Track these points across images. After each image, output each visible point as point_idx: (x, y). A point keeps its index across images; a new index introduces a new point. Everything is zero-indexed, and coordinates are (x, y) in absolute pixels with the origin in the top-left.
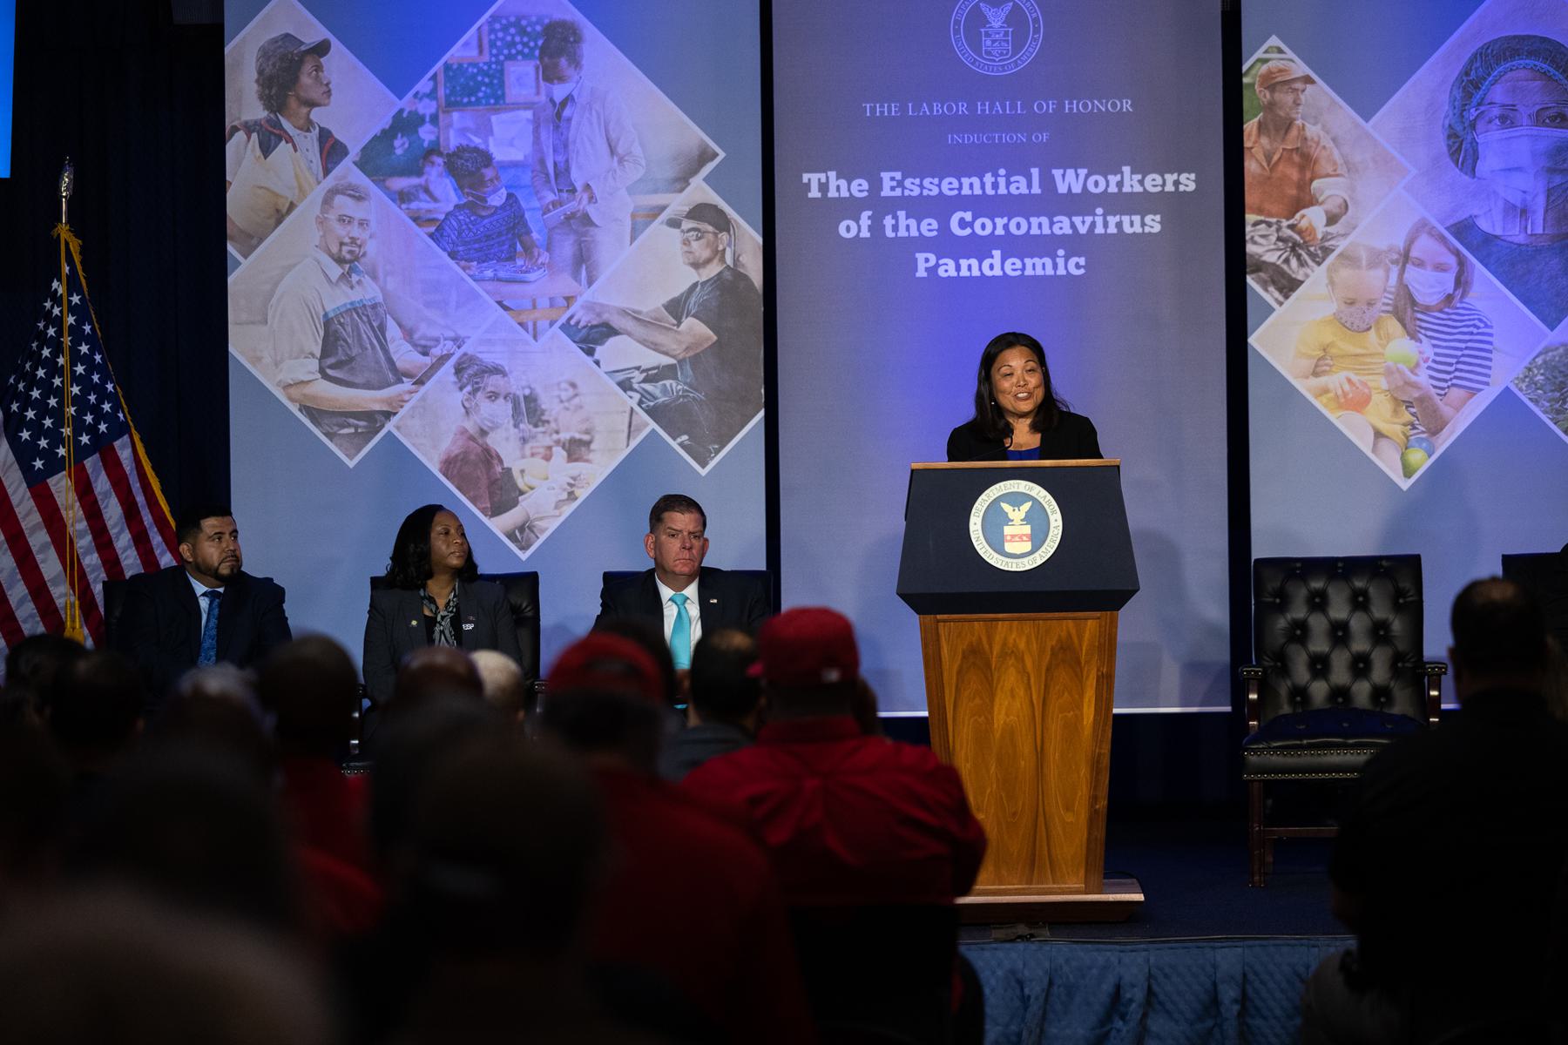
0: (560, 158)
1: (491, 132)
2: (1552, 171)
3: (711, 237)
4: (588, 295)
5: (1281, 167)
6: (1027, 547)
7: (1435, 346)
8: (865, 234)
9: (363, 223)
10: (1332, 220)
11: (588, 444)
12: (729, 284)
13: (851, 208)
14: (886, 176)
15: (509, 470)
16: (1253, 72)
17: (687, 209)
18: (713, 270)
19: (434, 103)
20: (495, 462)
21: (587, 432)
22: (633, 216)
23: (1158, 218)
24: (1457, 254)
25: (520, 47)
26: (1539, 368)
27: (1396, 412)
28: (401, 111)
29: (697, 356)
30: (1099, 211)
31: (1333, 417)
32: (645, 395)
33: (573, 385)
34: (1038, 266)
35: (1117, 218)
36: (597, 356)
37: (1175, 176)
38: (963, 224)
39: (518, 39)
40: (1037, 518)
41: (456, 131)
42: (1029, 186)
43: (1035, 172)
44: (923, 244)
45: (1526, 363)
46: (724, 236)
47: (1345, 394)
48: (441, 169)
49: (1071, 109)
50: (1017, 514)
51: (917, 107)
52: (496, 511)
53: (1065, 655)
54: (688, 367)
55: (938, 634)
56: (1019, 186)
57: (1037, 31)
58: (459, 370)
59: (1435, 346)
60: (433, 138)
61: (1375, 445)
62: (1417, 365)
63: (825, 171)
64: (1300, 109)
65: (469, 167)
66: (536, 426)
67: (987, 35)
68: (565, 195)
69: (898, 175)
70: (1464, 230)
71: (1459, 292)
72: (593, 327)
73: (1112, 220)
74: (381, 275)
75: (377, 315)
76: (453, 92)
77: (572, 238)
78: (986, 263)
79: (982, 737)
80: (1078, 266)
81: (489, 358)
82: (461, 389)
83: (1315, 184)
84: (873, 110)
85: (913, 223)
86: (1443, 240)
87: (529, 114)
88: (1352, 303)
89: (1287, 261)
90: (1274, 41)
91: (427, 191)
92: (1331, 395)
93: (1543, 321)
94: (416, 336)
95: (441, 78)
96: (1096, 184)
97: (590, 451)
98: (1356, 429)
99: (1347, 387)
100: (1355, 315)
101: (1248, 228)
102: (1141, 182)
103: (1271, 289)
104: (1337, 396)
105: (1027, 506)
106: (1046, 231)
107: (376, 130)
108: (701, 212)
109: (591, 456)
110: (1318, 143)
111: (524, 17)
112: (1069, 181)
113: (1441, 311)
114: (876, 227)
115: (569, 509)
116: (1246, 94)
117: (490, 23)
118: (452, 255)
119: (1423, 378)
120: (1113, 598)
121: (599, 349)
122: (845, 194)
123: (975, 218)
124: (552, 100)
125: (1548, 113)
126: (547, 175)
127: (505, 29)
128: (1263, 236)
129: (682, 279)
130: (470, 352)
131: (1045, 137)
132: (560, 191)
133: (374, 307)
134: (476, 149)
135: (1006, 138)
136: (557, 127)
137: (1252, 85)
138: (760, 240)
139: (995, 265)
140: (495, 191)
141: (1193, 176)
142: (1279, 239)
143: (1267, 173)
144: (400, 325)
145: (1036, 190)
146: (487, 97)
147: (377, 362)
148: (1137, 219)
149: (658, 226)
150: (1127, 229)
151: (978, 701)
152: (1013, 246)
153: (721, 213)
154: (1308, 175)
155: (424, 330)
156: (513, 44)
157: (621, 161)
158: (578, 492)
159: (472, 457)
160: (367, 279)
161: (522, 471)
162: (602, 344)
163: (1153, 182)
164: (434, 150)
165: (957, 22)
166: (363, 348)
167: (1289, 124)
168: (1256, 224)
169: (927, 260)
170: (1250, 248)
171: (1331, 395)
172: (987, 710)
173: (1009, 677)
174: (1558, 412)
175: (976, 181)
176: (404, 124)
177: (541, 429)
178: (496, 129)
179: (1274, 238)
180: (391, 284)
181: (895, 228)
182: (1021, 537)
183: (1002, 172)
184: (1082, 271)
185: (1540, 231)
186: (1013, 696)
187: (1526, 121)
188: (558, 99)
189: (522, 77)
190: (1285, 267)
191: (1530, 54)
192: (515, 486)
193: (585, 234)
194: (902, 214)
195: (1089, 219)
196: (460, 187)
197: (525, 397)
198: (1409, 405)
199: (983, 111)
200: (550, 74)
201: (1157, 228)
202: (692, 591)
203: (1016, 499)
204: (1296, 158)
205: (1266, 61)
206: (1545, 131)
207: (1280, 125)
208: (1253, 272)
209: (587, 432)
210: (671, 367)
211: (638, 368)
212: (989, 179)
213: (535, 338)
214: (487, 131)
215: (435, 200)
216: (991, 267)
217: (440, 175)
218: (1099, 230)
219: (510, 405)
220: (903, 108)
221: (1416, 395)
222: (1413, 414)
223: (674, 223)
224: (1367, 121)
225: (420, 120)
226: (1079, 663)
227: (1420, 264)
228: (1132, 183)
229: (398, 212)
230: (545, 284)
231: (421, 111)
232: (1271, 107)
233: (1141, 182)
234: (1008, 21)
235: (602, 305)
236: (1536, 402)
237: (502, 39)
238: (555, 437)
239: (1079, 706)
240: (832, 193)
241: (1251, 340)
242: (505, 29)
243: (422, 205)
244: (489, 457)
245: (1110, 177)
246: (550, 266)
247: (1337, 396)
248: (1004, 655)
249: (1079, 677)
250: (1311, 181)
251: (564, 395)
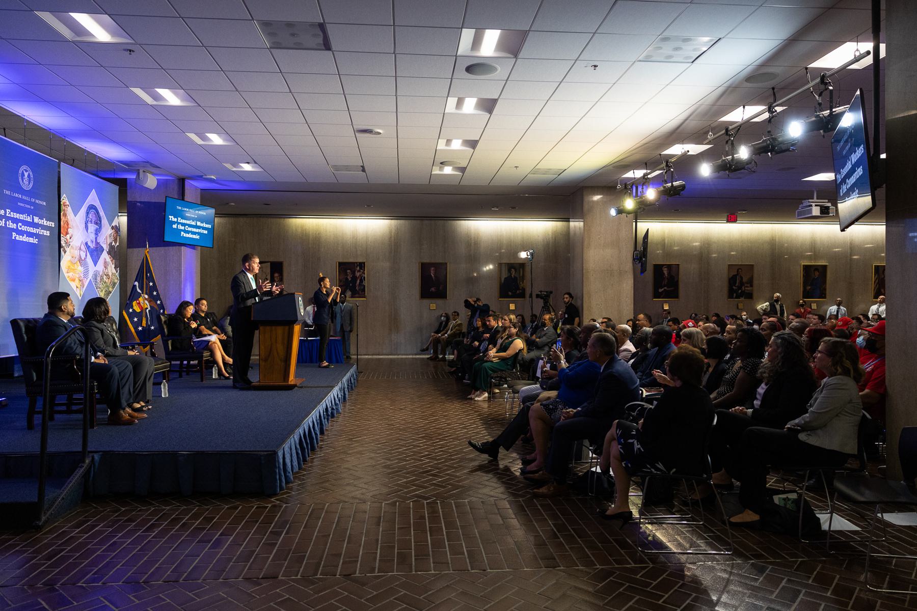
34: (31, 240)
56: (29, 219)
70: (86, 244)
112: (36, 220)
114: (5, 224)
139: (24, 239)
207: (65, 215)
228: (45, 222)
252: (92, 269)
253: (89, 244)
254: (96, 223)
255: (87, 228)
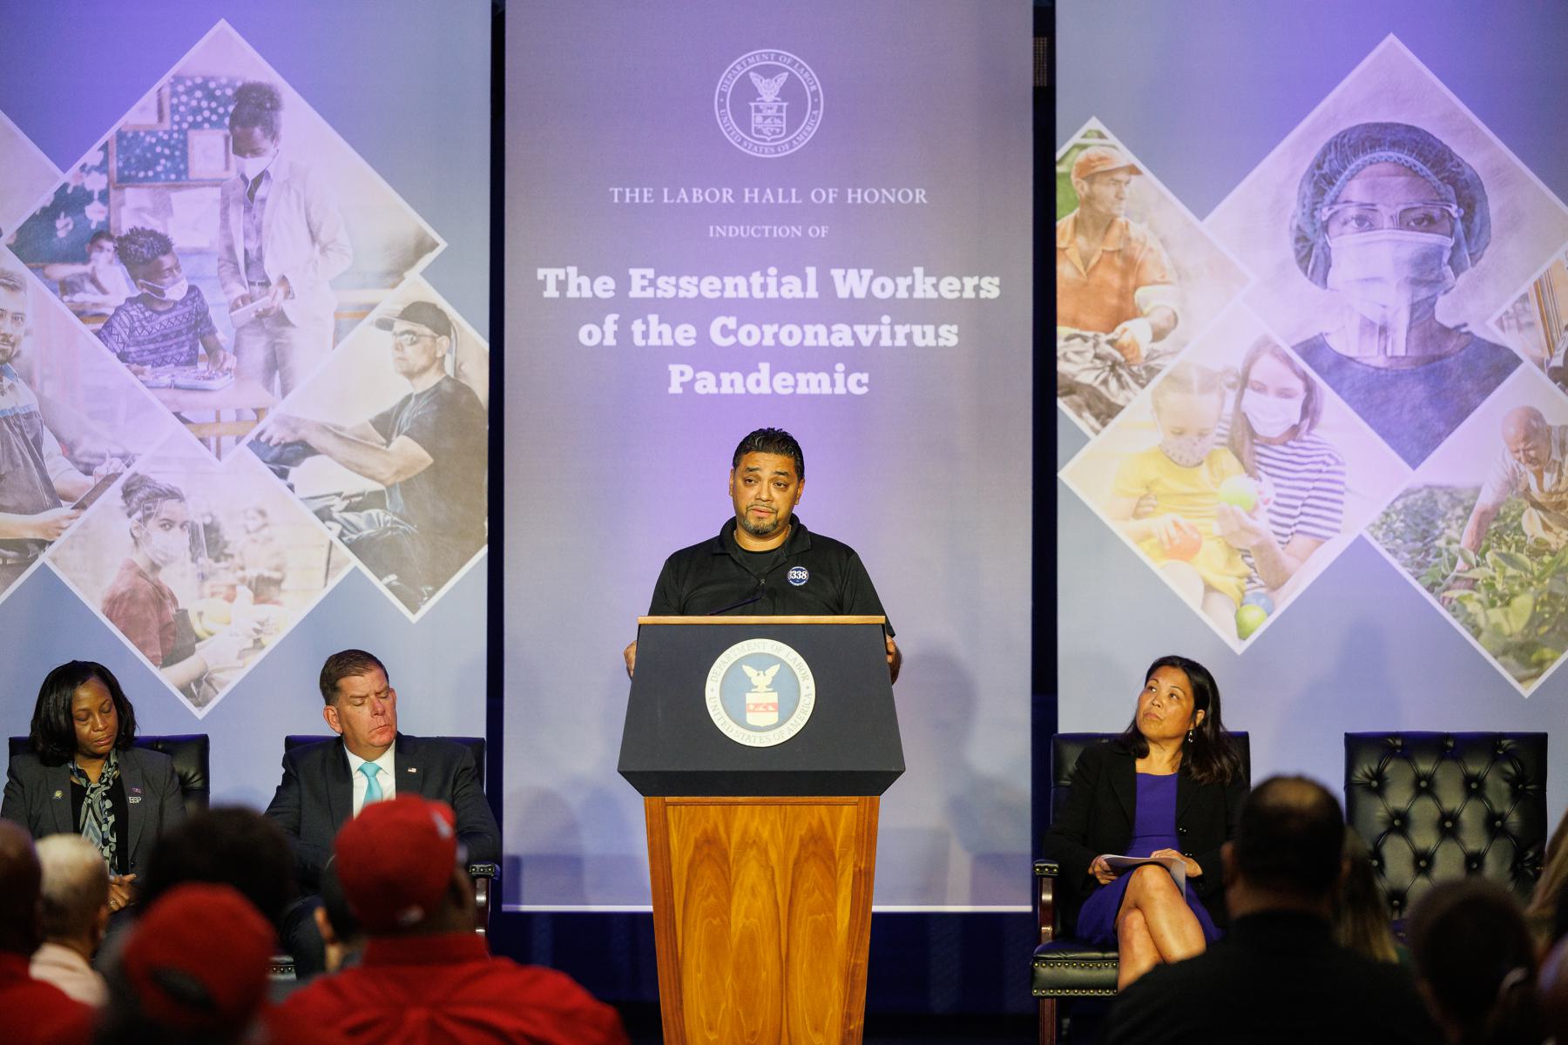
0: (252, 246)
1: (171, 211)
2: (1416, 282)
3: (428, 341)
4: (280, 408)
5: (1099, 272)
6: (773, 718)
7: (1277, 485)
8: (610, 341)
9: (17, 317)
10: (1158, 335)
11: (278, 582)
12: (448, 398)
13: (594, 310)
14: (635, 273)
15: (183, 614)
16: (1069, 159)
17: (400, 308)
18: (430, 380)
19: (104, 178)
20: (168, 602)
21: (278, 569)
22: (337, 315)
23: (955, 329)
24: (1304, 377)
25: (206, 114)
26: (1398, 513)
27: (1229, 562)
28: (65, 186)
29: (408, 482)
30: (886, 319)
31: (1159, 566)
32: (347, 527)
33: (262, 513)
35: (907, 328)
36: (291, 479)
37: (976, 280)
38: (725, 331)
39: (204, 104)
40: (785, 685)
41: (133, 210)
42: (804, 288)
43: (811, 272)
44: (677, 354)
45: (1383, 508)
46: (444, 340)
47: (1171, 540)
48: (110, 255)
49: (854, 199)
50: (761, 679)
51: (674, 194)
52: (169, 660)
53: (817, 846)
54: (398, 495)
55: (666, 820)
56: (792, 288)
57: (816, 106)
58: (127, 493)
59: (1277, 485)
60: (102, 218)
61: (1205, 600)
62: (1256, 507)
63: (564, 266)
64: (1124, 204)
65: (145, 254)
66: (217, 560)
67: (758, 110)
68: (257, 289)
69: (650, 273)
70: (1312, 350)
71: (1307, 422)
72: (287, 445)
73: (901, 330)
74: (37, 380)
75: (31, 425)
76: (127, 165)
77: (264, 339)
78: (752, 378)
79: (717, 943)
80: (860, 384)
81: (163, 479)
82: (129, 515)
83: (1140, 293)
84: (622, 195)
85: (666, 328)
86: (1288, 360)
87: (216, 193)
88: (1180, 433)
89: (1105, 382)
90: (1094, 124)
91: (94, 281)
92: (1155, 540)
93: (1406, 457)
94: (77, 452)
95: (113, 148)
96: (883, 288)
97: (280, 590)
98: (1182, 580)
99: (1173, 532)
100: (1184, 449)
101: (1060, 343)
102: (936, 287)
103: (1086, 414)
104: (1161, 542)
105: (774, 669)
106: (823, 342)
107: (35, 208)
108: (415, 312)
109: (282, 597)
110: (1144, 244)
111: (213, 78)
113: (1285, 444)
114: (624, 333)
115: (255, 659)
116: (1060, 185)
117: (172, 85)
118: (123, 357)
119: (1263, 523)
120: (872, 782)
121: (293, 471)
122: (587, 293)
123: (740, 324)
124: (243, 177)
125: (1413, 214)
126: (236, 264)
127: (189, 92)
128: (1077, 353)
129: (394, 390)
130: (141, 472)
131: (823, 231)
132: (251, 284)
133: (29, 416)
134: (153, 233)
135: (777, 232)
136: (248, 209)
137: (1067, 175)
138: (485, 346)
140: (174, 283)
141: (996, 280)
142: (1097, 356)
143: (1084, 278)
144: (59, 439)
145: (812, 293)
146: (167, 171)
147: (31, 482)
148: (930, 329)
149: (366, 327)
150: (919, 342)
151: (712, 899)
152: (783, 359)
153: (440, 313)
154: (1132, 282)
155: (86, 446)
156: (199, 110)
157: (323, 250)
158: (264, 641)
159: (142, 596)
160: (21, 385)
161: (200, 614)
162: (297, 465)
163: (949, 287)
164: (103, 233)
165: (723, 95)
166: (14, 464)
167: (1110, 222)
168: (1069, 338)
169: (682, 374)
170: (1062, 367)
171: (1155, 540)
172: (722, 911)
173: (750, 874)
174: (1420, 565)
175: (741, 280)
176: (69, 201)
177: (223, 564)
178: (176, 207)
179: (1090, 355)
180: (49, 390)
181: (646, 335)
182: (766, 706)
183: (772, 271)
184: (864, 390)
185: (1401, 352)
186: (754, 893)
187: (1387, 222)
188: (251, 177)
189: (208, 149)
190: (1102, 389)
191: (1394, 145)
192: (191, 632)
193: (278, 336)
194: (653, 319)
195: (873, 329)
196: (134, 278)
197: (205, 526)
198: (1246, 554)
199: (751, 199)
200: (242, 146)
201: (953, 341)
202: (387, 761)
203: (761, 662)
204: (1118, 262)
205: (1084, 147)
206: (1409, 236)
208: (1065, 394)
209: (278, 569)
210: (379, 495)
211: (339, 495)
212: (756, 278)
213: (218, 456)
214: (165, 209)
215: (104, 292)
216: (758, 383)
217: (110, 262)
218: (886, 341)
219: (187, 536)
220: (658, 195)
221: (1254, 542)
222: (1251, 566)
223: (385, 325)
224: (1201, 214)
225: (87, 197)
226: (832, 855)
227: (1261, 389)
228: (924, 286)
229: (59, 306)
230: (228, 392)
231: (88, 188)
232: (1089, 200)
233: (936, 287)
234: (784, 93)
235: (298, 419)
236: (1394, 552)
237: (186, 104)
238: (240, 574)
239: (832, 908)
240: (572, 293)
241: (1061, 475)
242: (189, 92)
243: (88, 296)
244: (161, 597)
245: (900, 280)
246: (237, 372)
247: (1161, 542)
248: (744, 845)
249: (831, 872)
250: (1135, 288)
251: (252, 525)
252: (1368, 477)
253: (1344, 342)
254: (1427, 223)
255: (1312, 255)
